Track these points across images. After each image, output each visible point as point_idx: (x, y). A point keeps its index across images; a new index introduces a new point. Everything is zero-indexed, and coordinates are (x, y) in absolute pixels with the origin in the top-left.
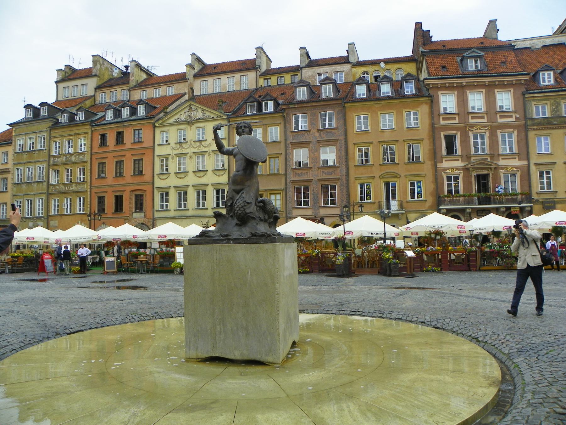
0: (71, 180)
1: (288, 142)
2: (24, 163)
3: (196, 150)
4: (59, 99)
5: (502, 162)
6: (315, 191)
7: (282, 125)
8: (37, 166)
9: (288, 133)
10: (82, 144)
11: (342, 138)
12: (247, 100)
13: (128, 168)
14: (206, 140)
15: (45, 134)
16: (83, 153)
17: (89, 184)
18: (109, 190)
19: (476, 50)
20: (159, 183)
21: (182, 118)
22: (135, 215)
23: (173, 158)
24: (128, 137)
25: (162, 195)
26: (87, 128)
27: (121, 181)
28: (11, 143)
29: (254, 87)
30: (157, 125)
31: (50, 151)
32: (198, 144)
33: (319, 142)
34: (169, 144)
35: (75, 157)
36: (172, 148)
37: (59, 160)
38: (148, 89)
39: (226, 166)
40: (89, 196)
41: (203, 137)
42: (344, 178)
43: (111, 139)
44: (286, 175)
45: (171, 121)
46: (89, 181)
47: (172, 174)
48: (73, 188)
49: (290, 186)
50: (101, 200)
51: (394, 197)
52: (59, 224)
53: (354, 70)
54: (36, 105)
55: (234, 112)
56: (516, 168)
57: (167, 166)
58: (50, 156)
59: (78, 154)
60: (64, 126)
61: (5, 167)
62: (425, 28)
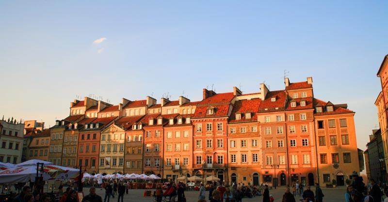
4: (71, 115)
5: (217, 151)
11: (162, 141)
15: (62, 133)
20: (101, 155)
22: (92, 167)
24: (92, 136)
29: (145, 114)
37: (67, 144)
43: (86, 137)
45: (106, 131)
48: (71, 156)
49: (144, 158)
50: (81, 161)
51: (178, 164)
54: (61, 120)
56: (223, 153)
62: (209, 89)
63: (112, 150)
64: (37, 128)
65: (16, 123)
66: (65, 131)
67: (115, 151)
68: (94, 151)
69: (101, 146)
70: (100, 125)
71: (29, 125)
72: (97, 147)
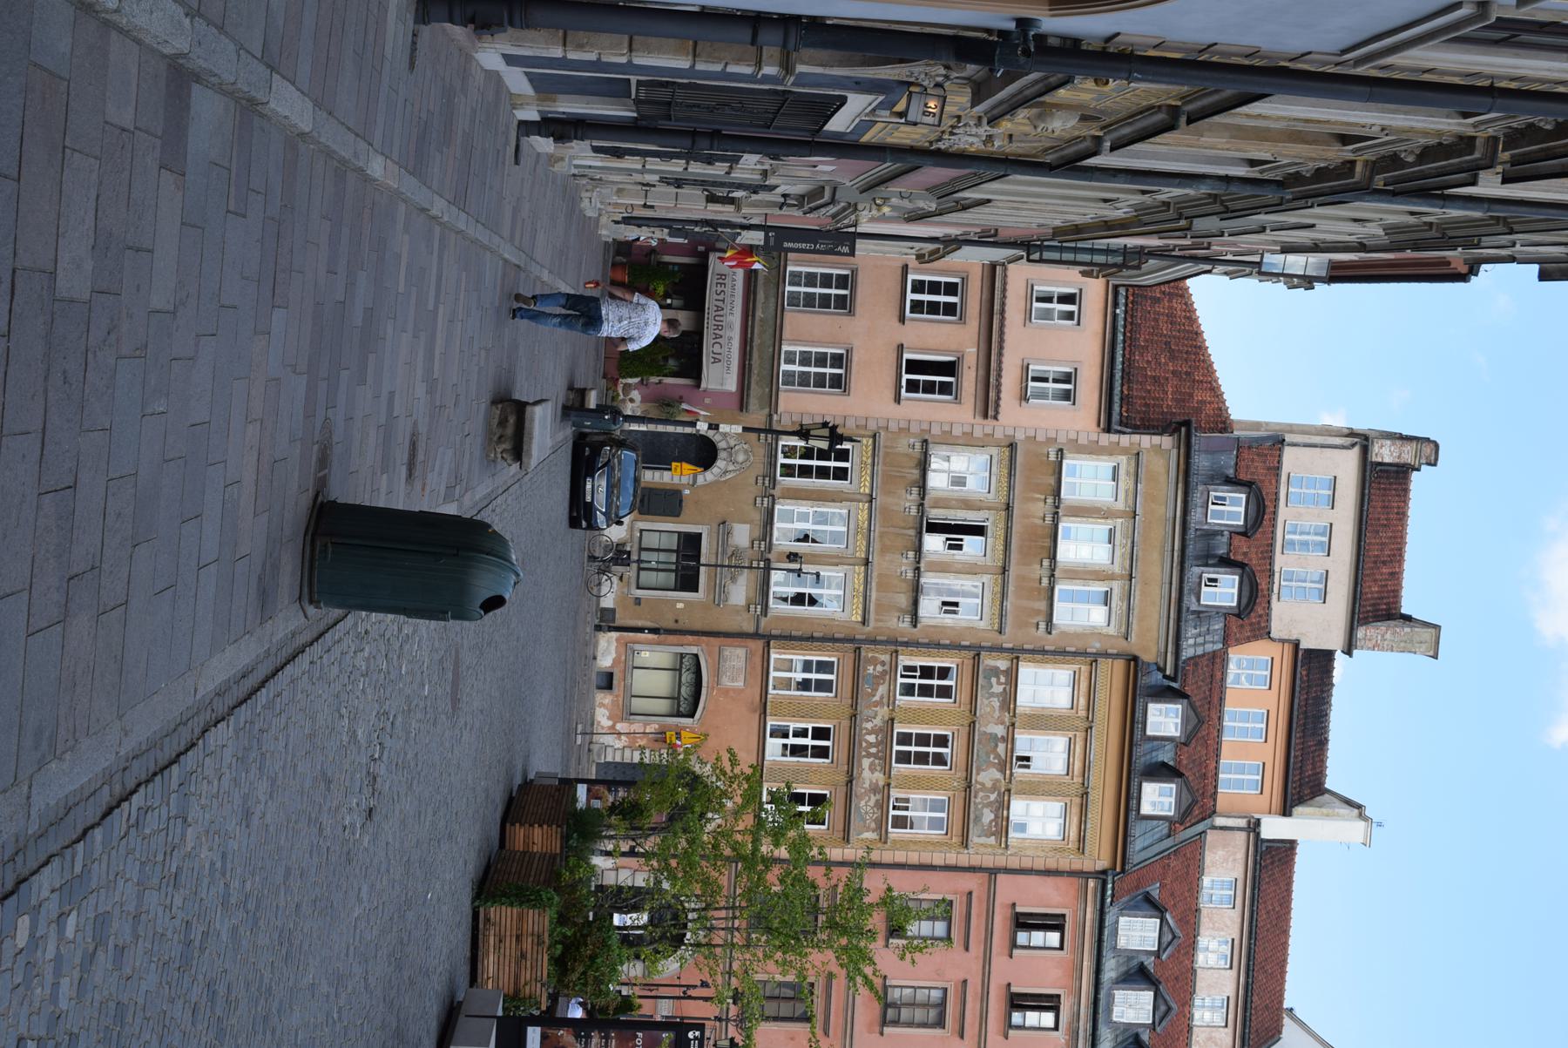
2: (1008, 507)
8: (986, 578)
10: (1039, 821)
16: (1001, 828)
26: (1099, 857)
28: (1108, 430)
31: (1042, 654)
35: (994, 788)
37: (989, 705)
38: (1235, 915)
46: (887, 857)
48: (869, 775)
52: (726, 692)
58: (1016, 654)
59: (1002, 806)
60: (1132, 722)
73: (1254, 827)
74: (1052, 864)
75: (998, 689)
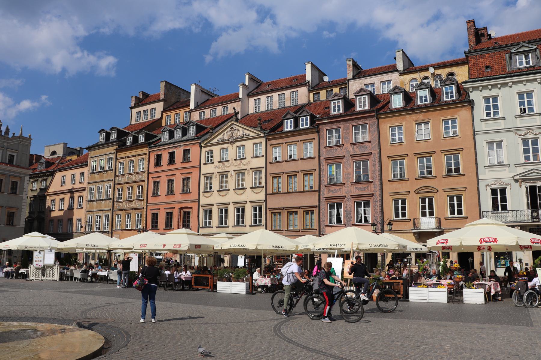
0: (131, 198)
1: (322, 158)
3: (236, 168)
6: (348, 208)
7: (316, 141)
9: (322, 149)
11: (376, 152)
12: (285, 117)
13: (178, 186)
14: (245, 158)
15: (113, 156)
16: (142, 172)
17: (145, 201)
18: (162, 207)
19: (527, 45)
20: (204, 201)
21: (226, 137)
23: (216, 177)
25: (206, 211)
26: (146, 150)
27: (172, 199)
28: (87, 165)
30: (203, 145)
32: (238, 162)
33: (352, 156)
34: (213, 163)
35: (135, 176)
36: (216, 167)
39: (263, 184)
40: (145, 213)
41: (243, 156)
42: (378, 194)
44: (319, 191)
45: (215, 141)
46: (145, 199)
47: (215, 192)
48: (133, 205)
49: (324, 203)
50: (155, 216)
51: (431, 214)
53: (402, 77)
55: (273, 130)
57: (211, 184)
59: (138, 173)
61: (81, 186)
63: (232, 184)
64: (68, 158)
65: (10, 136)
66: (118, 151)
67: (240, 188)
68: (185, 191)
69: (202, 177)
70: (199, 128)
71: (54, 153)
72: (193, 183)
73: (190, 112)
74: (147, 160)
75: (120, 178)
